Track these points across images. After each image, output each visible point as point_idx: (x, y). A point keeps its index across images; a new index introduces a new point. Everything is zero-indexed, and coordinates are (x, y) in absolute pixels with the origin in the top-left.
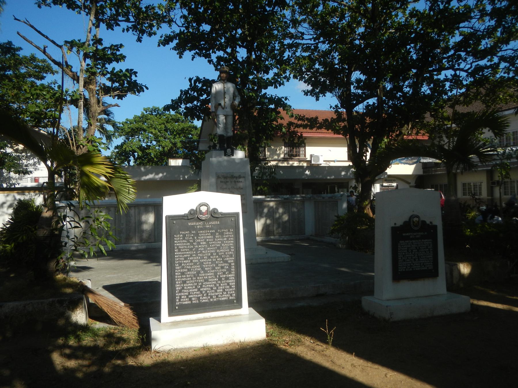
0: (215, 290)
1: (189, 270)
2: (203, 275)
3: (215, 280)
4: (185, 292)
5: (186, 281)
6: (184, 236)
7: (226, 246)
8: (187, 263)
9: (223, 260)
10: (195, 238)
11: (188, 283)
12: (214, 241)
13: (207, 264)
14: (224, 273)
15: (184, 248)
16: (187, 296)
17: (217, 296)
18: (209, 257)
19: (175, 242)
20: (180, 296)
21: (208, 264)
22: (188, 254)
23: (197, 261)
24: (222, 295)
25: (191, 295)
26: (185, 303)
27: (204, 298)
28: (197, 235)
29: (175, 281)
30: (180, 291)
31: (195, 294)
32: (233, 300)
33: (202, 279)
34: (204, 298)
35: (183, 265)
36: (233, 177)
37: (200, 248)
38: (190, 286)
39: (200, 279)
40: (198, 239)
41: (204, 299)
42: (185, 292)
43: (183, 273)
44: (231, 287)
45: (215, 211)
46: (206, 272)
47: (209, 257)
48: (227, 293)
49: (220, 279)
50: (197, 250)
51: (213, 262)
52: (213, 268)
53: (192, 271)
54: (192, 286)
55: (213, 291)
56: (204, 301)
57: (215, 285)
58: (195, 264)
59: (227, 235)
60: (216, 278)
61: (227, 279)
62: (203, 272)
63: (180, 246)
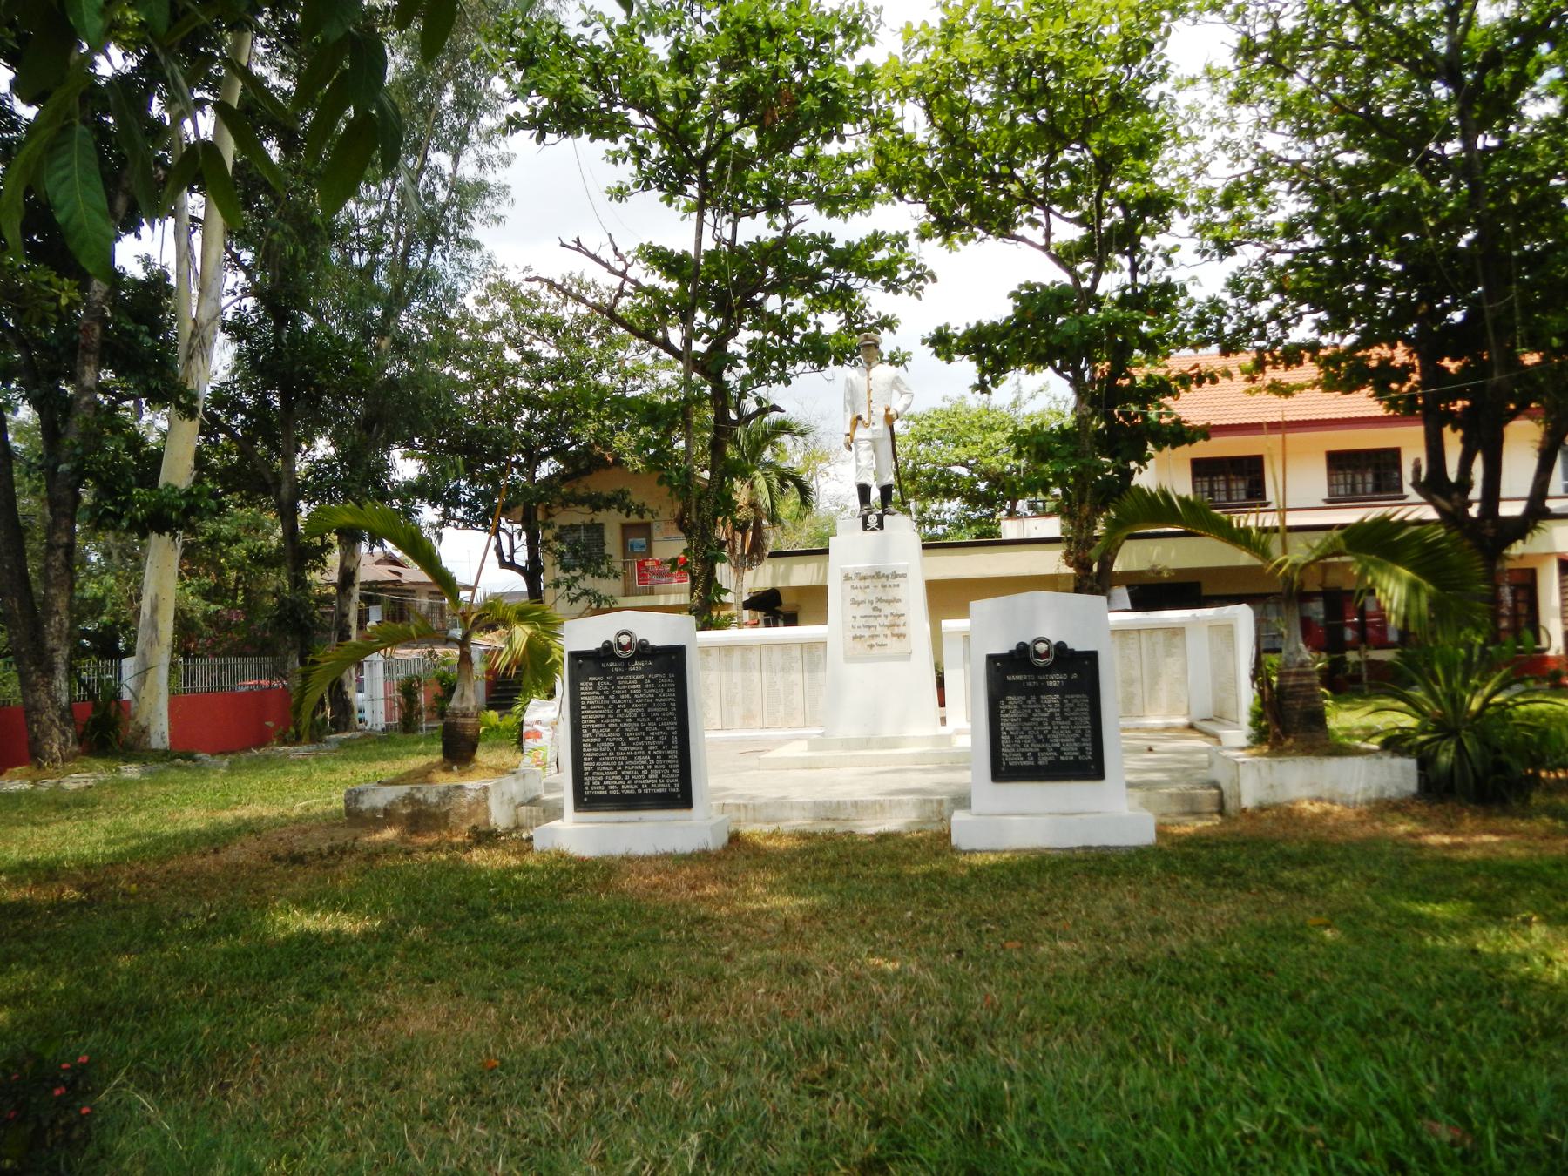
1: (604, 740)
14: (660, 747)
18: (634, 720)
28: (614, 682)
30: (590, 774)
36: (878, 576)
39: (621, 756)
46: (630, 744)
49: (653, 757)
52: (642, 739)
58: (613, 730)
61: (665, 757)
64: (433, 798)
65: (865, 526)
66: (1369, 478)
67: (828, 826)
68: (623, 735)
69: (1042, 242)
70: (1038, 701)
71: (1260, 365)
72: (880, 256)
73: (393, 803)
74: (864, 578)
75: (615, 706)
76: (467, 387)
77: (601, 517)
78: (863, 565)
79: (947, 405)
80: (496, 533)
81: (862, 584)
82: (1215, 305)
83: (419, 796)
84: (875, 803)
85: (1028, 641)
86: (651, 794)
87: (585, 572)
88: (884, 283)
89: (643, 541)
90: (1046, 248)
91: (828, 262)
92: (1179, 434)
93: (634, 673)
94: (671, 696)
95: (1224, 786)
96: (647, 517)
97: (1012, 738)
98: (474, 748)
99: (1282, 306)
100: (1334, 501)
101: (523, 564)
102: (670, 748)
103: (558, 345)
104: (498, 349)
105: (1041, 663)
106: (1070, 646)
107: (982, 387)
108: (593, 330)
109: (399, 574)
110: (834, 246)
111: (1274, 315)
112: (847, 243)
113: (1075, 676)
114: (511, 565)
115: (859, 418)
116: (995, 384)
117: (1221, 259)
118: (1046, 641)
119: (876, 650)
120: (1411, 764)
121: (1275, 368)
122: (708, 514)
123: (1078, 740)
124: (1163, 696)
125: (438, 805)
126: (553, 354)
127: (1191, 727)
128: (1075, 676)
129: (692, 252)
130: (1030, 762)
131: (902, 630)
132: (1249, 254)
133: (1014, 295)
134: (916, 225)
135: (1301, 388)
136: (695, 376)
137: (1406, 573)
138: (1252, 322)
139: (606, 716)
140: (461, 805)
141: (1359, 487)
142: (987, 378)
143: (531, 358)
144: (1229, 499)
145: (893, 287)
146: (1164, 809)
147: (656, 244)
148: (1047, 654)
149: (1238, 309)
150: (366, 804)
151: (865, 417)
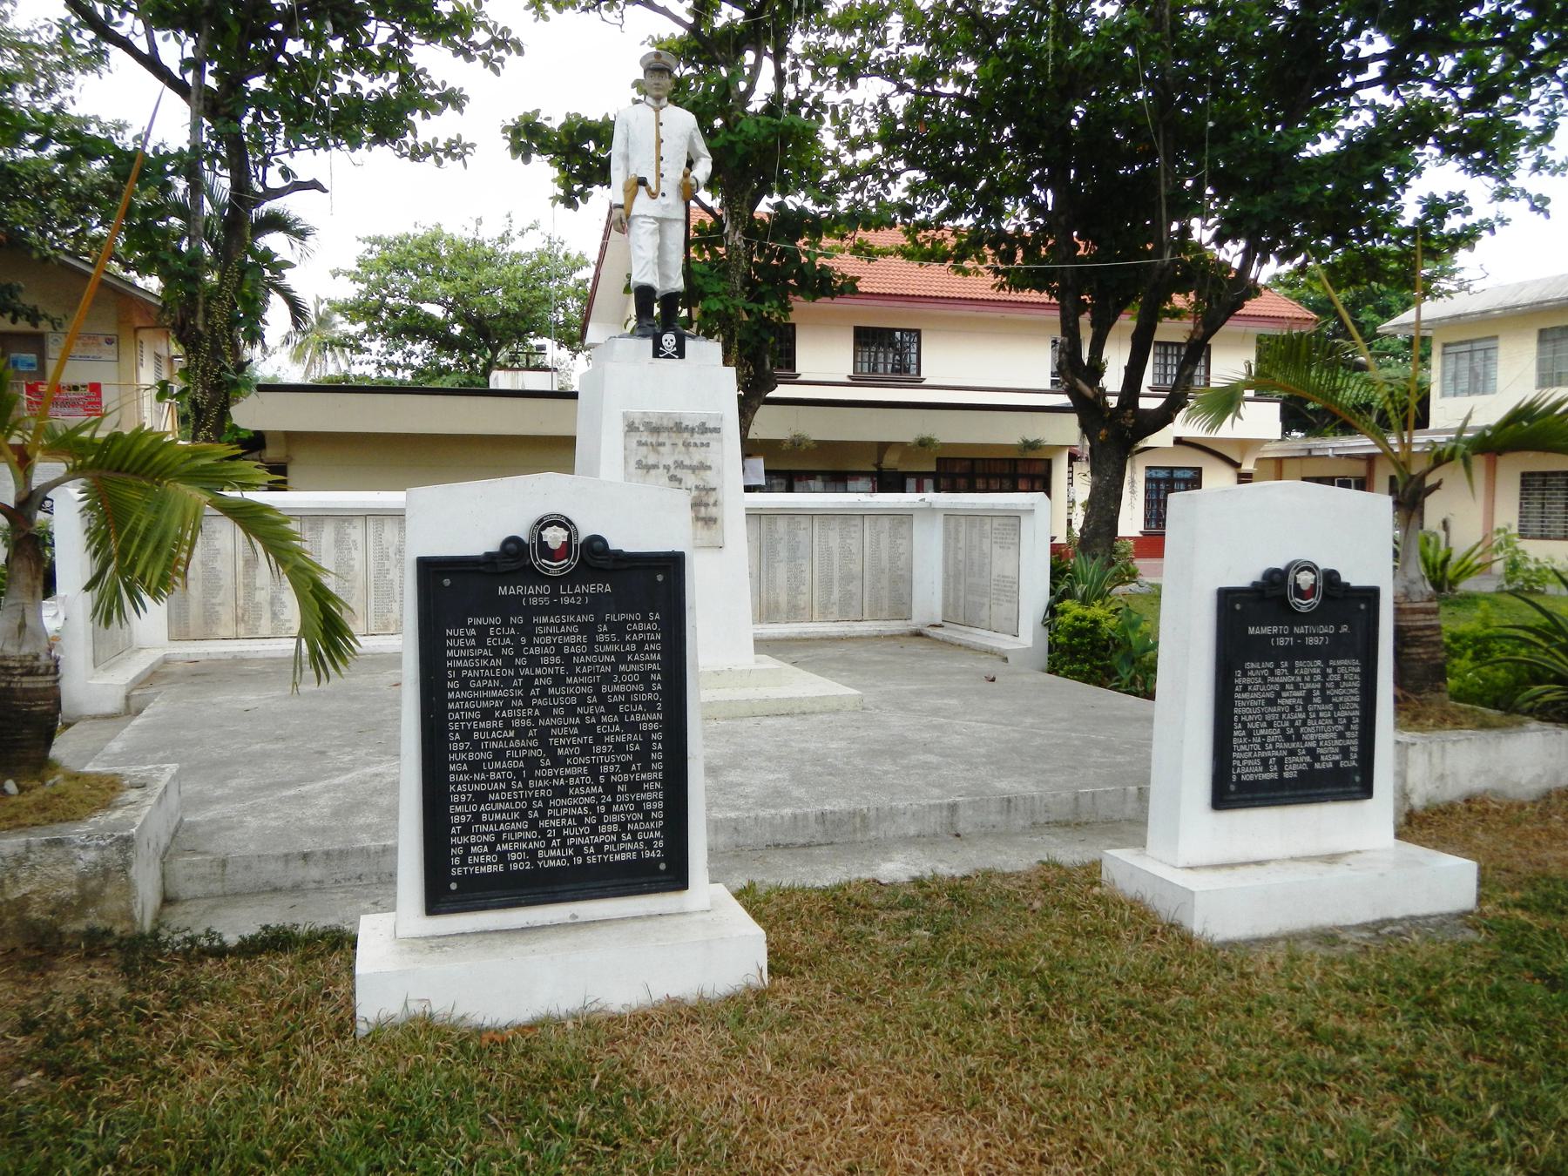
0: (591, 825)
1: (499, 755)
2: (550, 772)
3: (594, 790)
4: (486, 833)
5: (487, 792)
6: (482, 632)
7: (633, 672)
8: (490, 731)
9: (621, 723)
10: (524, 641)
11: (494, 802)
12: (591, 652)
13: (566, 737)
14: (625, 768)
15: (481, 678)
16: (492, 846)
17: (599, 848)
18: (570, 711)
19: (450, 653)
20: (467, 847)
21: (569, 736)
22: (494, 699)
23: (529, 723)
24: (615, 844)
25: (507, 841)
26: (483, 869)
27: (552, 853)
28: (528, 630)
29: (448, 794)
30: (466, 830)
31: (521, 840)
32: (659, 860)
33: (546, 788)
34: (552, 853)
35: (476, 735)
36: (679, 428)
37: (538, 676)
38: (501, 811)
40: (530, 644)
41: (552, 858)
42: (486, 833)
43: (475, 767)
44: (647, 817)
45: (596, 545)
46: (558, 762)
47: (570, 711)
48: (634, 839)
50: (528, 682)
51: (585, 729)
52: (586, 750)
53: (511, 758)
54: (508, 811)
55: (585, 830)
56: (551, 863)
57: (592, 807)
58: (521, 733)
59: (637, 632)
60: (597, 783)
61: (635, 787)
62: (548, 763)
63: (468, 668)
65: (657, 352)
70: (1291, 670)
79: (421, 232)
81: (652, 439)
86: (604, 865)
89: (32, 357)
93: (574, 610)
94: (652, 660)
96: (44, 326)
97: (1250, 734)
98: (48, 737)
99: (879, 158)
102: (646, 768)
105: (1303, 605)
113: (1344, 629)
115: (642, 182)
118: (1311, 568)
122: (220, 322)
128: (1344, 629)
131: (713, 511)
135: (884, 253)
140: (60, 882)
141: (881, 368)
148: (1313, 590)
151: (651, 182)
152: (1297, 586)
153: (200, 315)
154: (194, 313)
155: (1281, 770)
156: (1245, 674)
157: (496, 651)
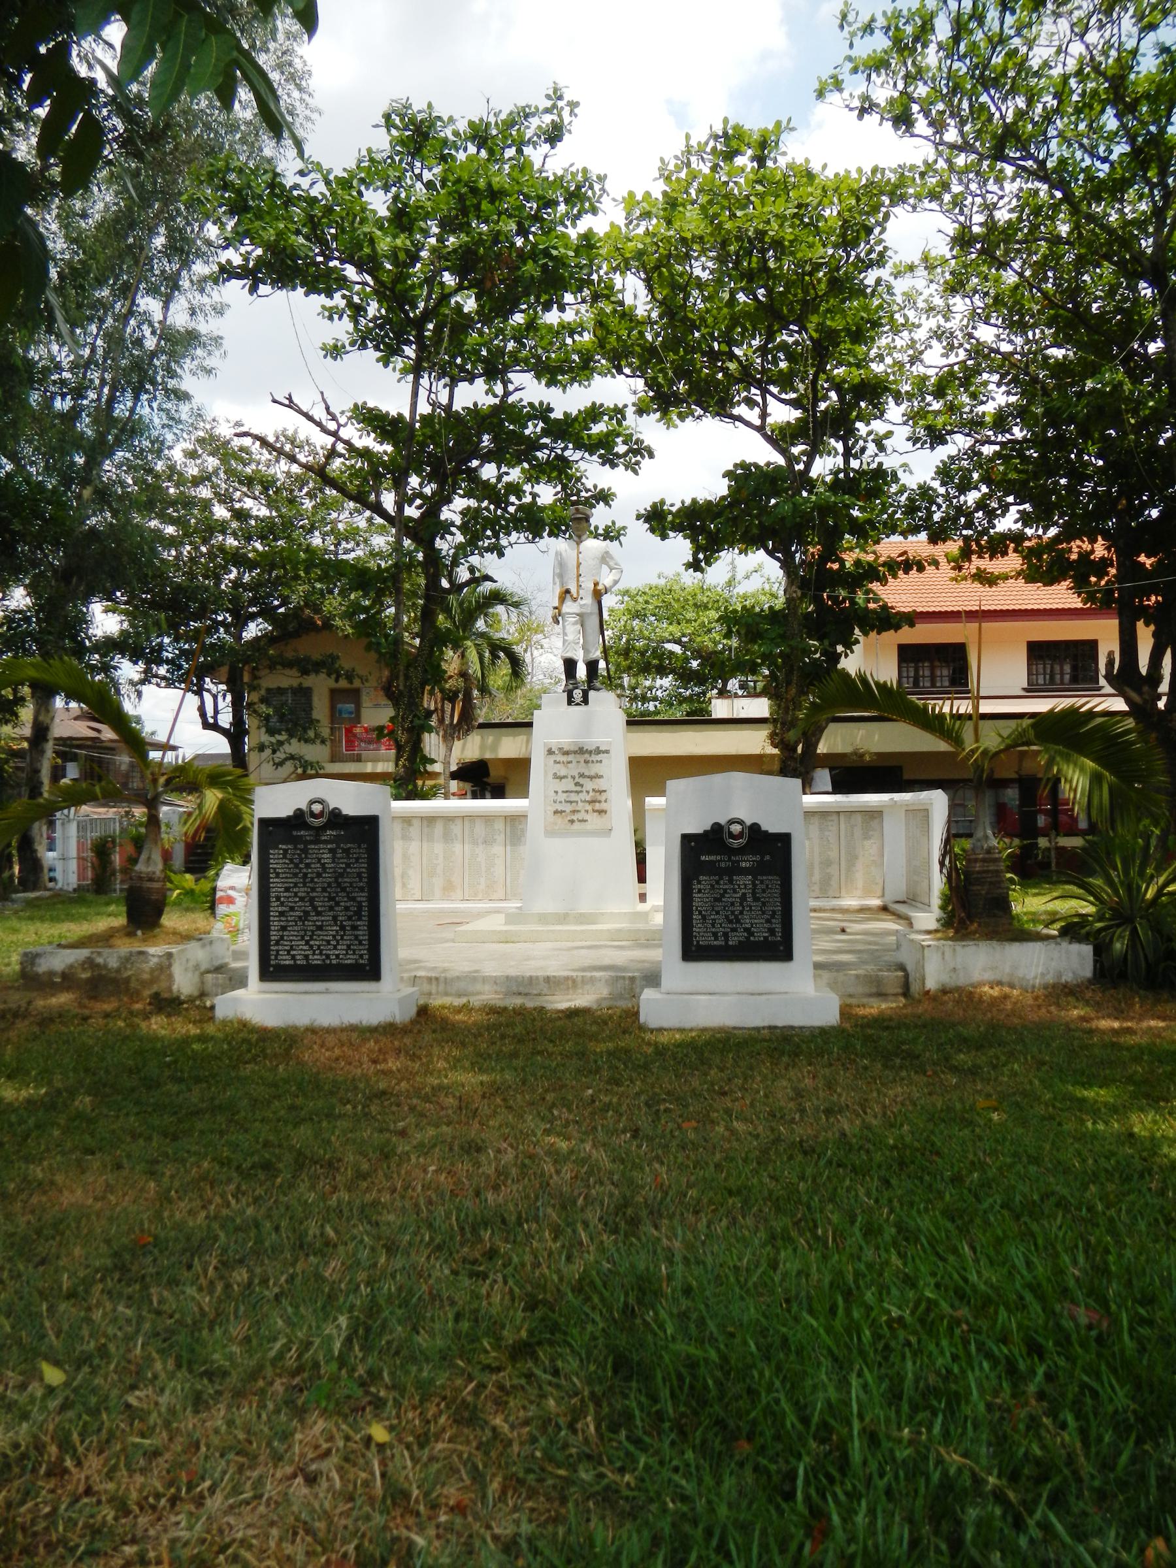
1: (292, 909)
14: (350, 918)
17: (337, 956)
18: (324, 890)
28: (305, 851)
30: (277, 943)
36: (581, 751)
44: (360, 943)
47: (324, 890)
49: (343, 928)
50: (305, 875)
52: (331, 908)
58: (302, 899)
61: (354, 928)
64: (113, 963)
65: (570, 701)
66: (1067, 668)
67: (518, 1001)
68: (312, 905)
69: (758, 422)
70: (731, 881)
71: (966, 554)
72: (598, 428)
73: (71, 966)
74: (567, 753)
75: (305, 875)
76: (172, 542)
77: (309, 681)
78: (566, 740)
79: (662, 582)
80: (199, 693)
81: (565, 758)
82: (925, 491)
83: (100, 960)
84: (567, 978)
85: (723, 821)
86: (338, 964)
87: (291, 736)
88: (600, 456)
89: (351, 707)
90: (760, 429)
91: (546, 433)
92: (887, 620)
93: (326, 842)
94: (363, 866)
95: (909, 968)
96: (357, 683)
97: (704, 917)
98: (160, 913)
99: (989, 496)
100: (1033, 690)
101: (227, 726)
102: (360, 919)
103: (269, 506)
104: (206, 505)
105: (736, 843)
106: (764, 828)
107: (695, 565)
108: (305, 490)
109: (98, 731)
110: (552, 416)
111: (981, 505)
112: (565, 414)
113: (767, 858)
114: (215, 727)
115: (568, 591)
116: (709, 564)
117: (932, 448)
118: (741, 822)
119: (577, 826)
120: (1087, 950)
121: (980, 557)
122: (416, 682)
123: (768, 921)
124: (860, 877)
125: (118, 971)
126: (264, 512)
127: (885, 909)
129: (407, 415)
130: (720, 942)
131: (603, 806)
132: (960, 442)
133: (728, 474)
134: (633, 399)
136: (407, 543)
137: (1090, 764)
138: (960, 511)
139: (296, 885)
140: (143, 971)
142: (701, 556)
143: (241, 515)
144: (933, 685)
145: (610, 461)
146: (851, 990)
147: (371, 405)
149: (947, 497)
150: (43, 967)
151: (574, 591)
152: (730, 833)
153: (402, 678)
154: (397, 678)
155: (727, 940)
156: (699, 882)
157: (291, 860)
